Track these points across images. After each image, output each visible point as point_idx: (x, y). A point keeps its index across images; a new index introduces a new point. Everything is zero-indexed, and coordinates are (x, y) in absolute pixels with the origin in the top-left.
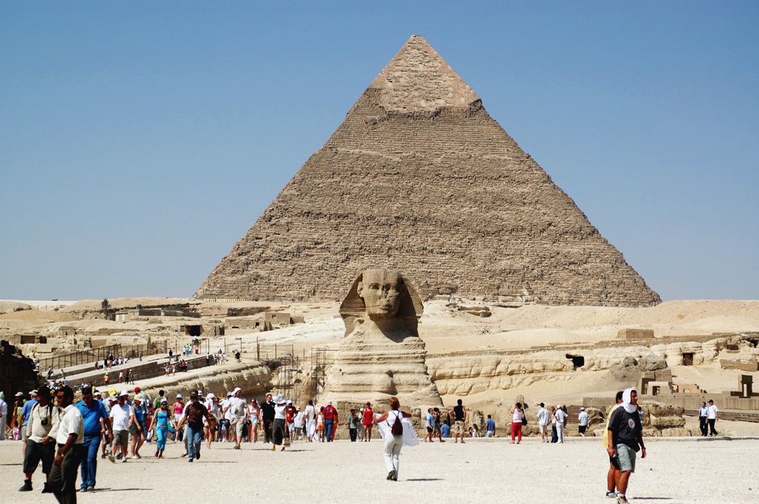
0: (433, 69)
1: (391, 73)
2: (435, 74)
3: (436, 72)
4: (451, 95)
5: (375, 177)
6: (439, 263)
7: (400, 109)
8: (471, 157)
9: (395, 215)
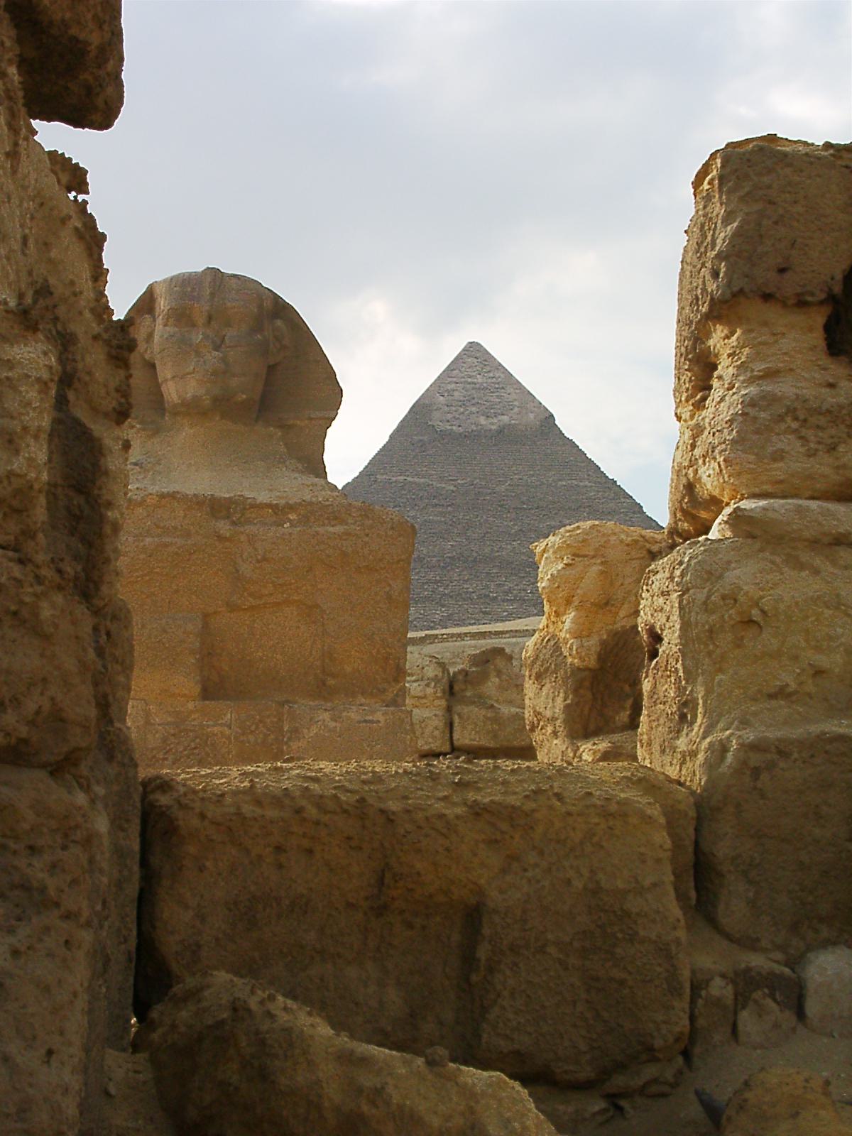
0: (494, 380)
1: (443, 385)
2: (497, 386)
3: (498, 383)
4: (516, 410)
5: (424, 508)
6: (505, 614)
7: (454, 428)
8: (543, 483)
9: (449, 555)
